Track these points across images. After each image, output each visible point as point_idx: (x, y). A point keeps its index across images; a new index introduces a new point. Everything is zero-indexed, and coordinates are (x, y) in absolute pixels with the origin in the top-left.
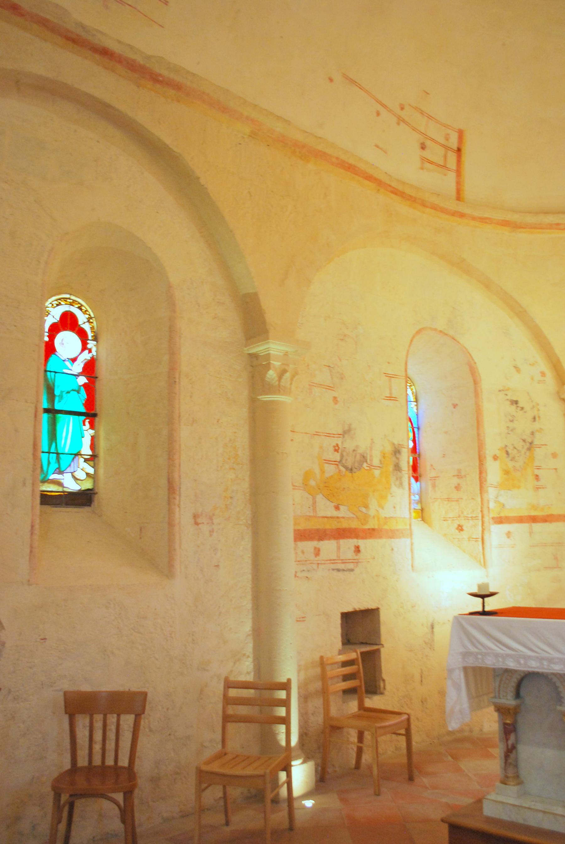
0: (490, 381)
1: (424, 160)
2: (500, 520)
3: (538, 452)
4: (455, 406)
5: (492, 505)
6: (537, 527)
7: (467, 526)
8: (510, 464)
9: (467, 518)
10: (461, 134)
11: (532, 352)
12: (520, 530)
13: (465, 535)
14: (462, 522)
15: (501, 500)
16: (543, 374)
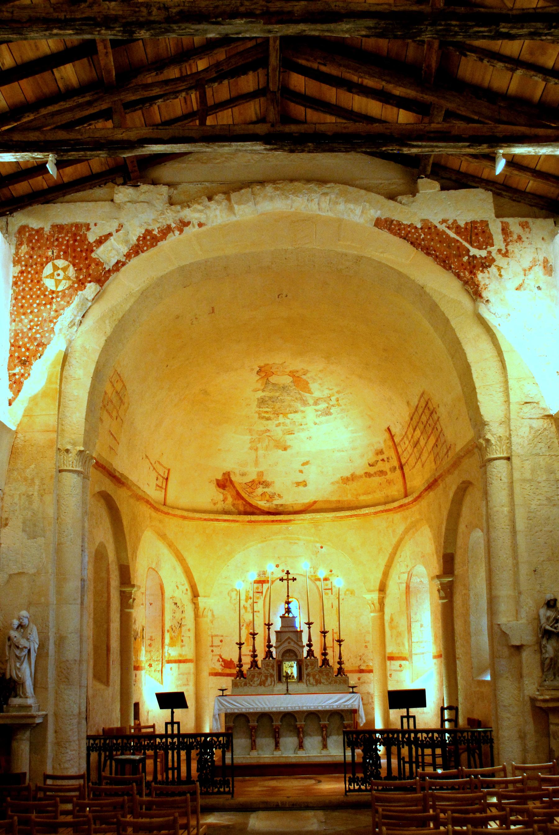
0: (167, 594)
1: (157, 485)
2: (169, 662)
3: (183, 629)
4: (151, 604)
5: (166, 654)
6: (181, 665)
7: (154, 664)
8: (173, 634)
9: (154, 661)
10: (169, 470)
11: (183, 579)
12: (174, 666)
13: (153, 669)
14: (152, 662)
15: (169, 652)
16: (187, 590)
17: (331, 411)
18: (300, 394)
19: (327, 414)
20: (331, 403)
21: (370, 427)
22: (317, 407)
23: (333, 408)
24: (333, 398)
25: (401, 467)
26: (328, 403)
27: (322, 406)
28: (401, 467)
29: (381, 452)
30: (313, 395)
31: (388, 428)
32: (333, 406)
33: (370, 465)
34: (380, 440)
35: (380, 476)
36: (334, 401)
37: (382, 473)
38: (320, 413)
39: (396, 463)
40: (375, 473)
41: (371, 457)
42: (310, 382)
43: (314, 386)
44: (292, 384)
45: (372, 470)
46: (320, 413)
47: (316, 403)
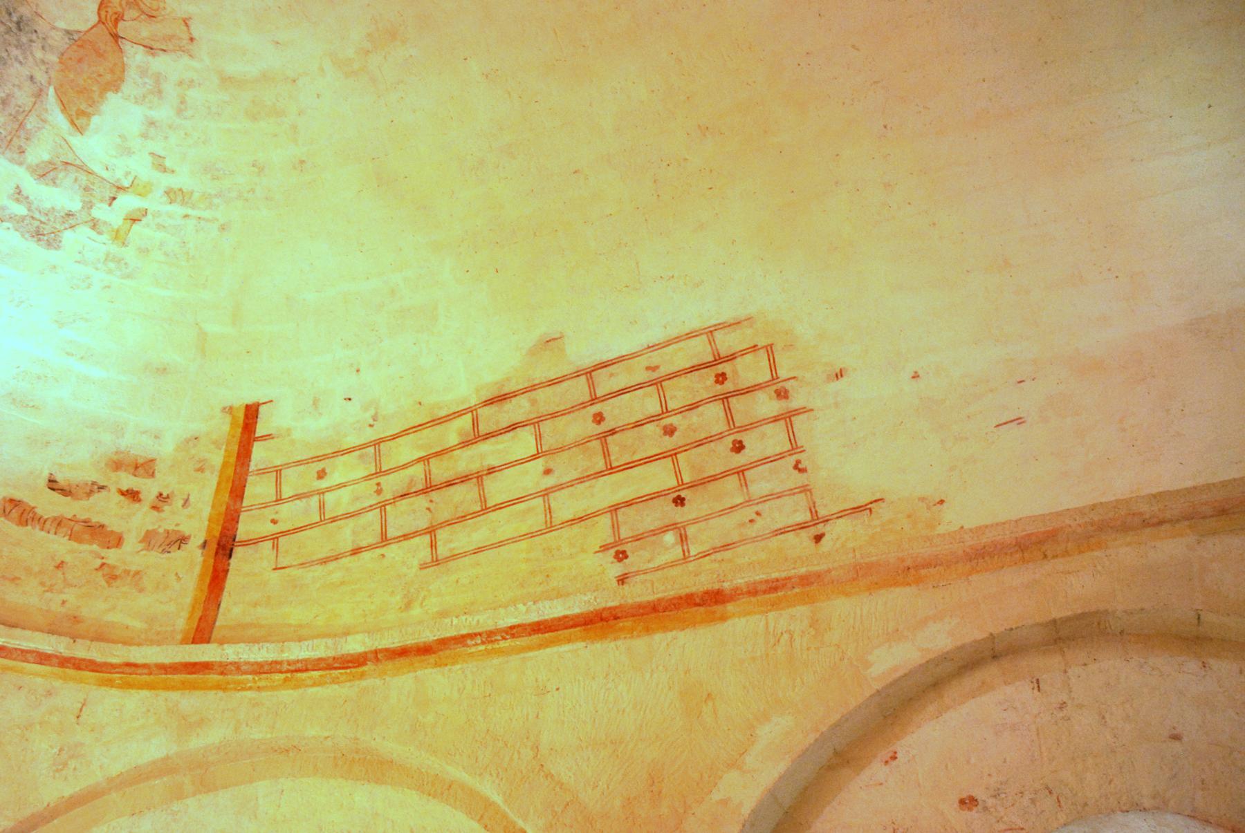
17: (67, 236)
18: (39, 94)
19: (38, 235)
20: (101, 211)
21: (163, 370)
22: (31, 186)
23: (84, 231)
24: (127, 202)
25: (223, 547)
26: (88, 206)
27: (60, 197)
28: (223, 547)
29: (145, 467)
30: (75, 140)
31: (252, 413)
32: (94, 224)
33: (52, 484)
34: (177, 428)
35: (72, 536)
36: (113, 216)
37: (96, 532)
38: (21, 210)
39: (197, 523)
40: (59, 522)
41: (79, 463)
42: (128, 88)
43: (120, 114)
44: (58, 40)
45: (51, 505)
46: (21, 210)
47: (45, 173)
